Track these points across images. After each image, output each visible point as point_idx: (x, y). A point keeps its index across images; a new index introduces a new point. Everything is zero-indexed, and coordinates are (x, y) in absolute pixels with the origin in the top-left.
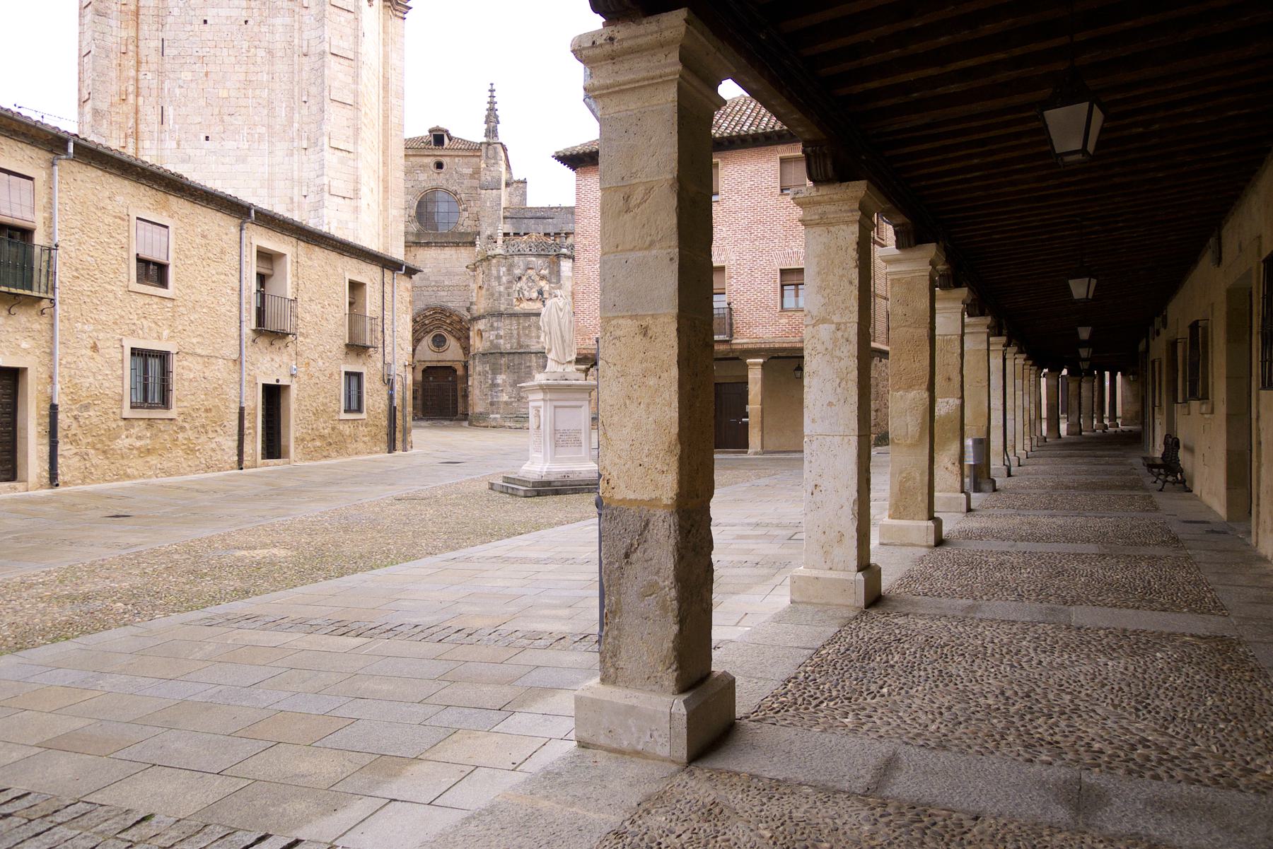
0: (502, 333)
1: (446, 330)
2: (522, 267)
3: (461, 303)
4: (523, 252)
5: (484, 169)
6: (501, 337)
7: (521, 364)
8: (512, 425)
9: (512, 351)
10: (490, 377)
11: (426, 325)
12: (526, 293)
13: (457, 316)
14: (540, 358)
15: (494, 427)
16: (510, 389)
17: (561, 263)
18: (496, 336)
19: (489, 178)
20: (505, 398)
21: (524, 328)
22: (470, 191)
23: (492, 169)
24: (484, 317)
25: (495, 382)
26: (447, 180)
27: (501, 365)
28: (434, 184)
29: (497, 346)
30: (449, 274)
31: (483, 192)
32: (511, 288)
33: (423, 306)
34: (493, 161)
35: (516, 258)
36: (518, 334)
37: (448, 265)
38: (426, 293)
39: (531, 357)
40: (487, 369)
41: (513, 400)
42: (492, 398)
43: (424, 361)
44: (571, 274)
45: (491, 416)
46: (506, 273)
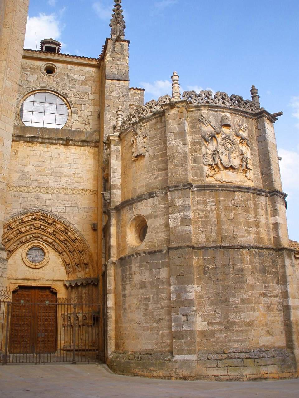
0: (191, 215)
3: (68, 209)
4: (214, 104)
5: (110, 62)
7: (227, 266)
8: (220, 372)
9: (209, 245)
11: (21, 233)
12: (222, 157)
13: (62, 223)
14: (254, 256)
15: (185, 378)
16: (209, 309)
19: (115, 71)
20: (200, 324)
23: (118, 63)
25: (184, 296)
26: (58, 83)
28: (44, 86)
29: (187, 237)
30: (55, 174)
32: (199, 150)
33: (20, 210)
35: (204, 112)
36: (218, 218)
37: (54, 165)
38: (26, 195)
39: (242, 255)
41: (216, 327)
42: (179, 325)
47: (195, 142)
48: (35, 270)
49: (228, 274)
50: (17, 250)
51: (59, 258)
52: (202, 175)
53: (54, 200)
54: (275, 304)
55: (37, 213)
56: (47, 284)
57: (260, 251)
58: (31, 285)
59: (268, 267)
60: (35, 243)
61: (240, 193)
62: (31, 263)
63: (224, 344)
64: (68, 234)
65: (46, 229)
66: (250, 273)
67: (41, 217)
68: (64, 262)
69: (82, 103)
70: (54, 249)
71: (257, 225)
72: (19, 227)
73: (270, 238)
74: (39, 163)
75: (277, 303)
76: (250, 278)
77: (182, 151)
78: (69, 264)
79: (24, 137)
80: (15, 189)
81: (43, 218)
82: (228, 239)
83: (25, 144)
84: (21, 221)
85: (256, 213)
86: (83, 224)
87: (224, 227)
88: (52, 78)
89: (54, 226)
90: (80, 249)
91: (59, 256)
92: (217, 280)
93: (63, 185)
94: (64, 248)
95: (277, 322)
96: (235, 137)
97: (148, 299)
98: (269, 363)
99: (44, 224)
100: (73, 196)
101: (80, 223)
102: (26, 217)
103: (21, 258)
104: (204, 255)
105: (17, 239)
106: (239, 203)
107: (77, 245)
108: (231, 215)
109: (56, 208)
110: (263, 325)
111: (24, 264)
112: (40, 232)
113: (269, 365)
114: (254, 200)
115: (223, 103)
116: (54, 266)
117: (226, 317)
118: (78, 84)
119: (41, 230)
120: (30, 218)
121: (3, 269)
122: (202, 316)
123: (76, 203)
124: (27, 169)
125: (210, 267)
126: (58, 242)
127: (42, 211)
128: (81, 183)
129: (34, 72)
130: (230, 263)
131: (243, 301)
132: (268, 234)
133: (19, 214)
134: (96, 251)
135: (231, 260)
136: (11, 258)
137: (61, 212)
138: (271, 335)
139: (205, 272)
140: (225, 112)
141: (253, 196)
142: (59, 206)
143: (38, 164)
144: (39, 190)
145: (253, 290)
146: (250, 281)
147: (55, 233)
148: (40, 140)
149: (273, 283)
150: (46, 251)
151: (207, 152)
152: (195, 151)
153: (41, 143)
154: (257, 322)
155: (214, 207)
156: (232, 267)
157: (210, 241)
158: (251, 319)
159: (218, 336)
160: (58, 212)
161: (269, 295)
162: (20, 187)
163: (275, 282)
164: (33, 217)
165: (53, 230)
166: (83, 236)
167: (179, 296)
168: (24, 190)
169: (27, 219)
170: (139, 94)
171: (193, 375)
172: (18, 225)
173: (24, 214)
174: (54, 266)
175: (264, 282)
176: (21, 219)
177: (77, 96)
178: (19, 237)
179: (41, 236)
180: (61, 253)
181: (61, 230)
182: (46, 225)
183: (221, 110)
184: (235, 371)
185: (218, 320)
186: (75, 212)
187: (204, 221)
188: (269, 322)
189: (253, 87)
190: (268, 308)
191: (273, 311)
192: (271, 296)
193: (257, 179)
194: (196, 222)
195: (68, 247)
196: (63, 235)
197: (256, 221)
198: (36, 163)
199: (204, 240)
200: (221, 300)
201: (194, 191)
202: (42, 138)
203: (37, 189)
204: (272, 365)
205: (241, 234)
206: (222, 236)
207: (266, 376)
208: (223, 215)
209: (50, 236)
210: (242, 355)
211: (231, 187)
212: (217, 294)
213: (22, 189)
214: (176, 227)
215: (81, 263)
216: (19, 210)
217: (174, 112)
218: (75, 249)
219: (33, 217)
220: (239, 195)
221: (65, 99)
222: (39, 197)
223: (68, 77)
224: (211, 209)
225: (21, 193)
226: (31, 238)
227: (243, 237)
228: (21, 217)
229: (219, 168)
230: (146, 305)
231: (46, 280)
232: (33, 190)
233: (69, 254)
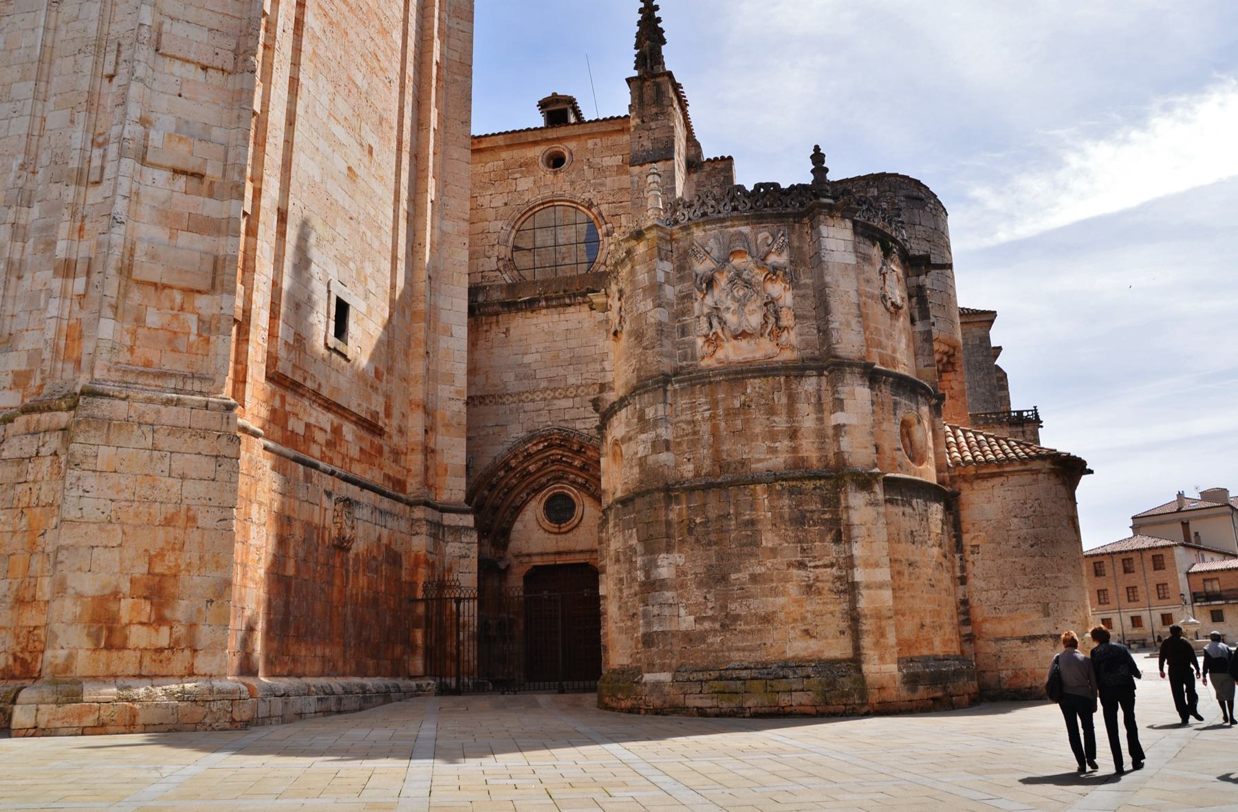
2: (715, 253)
4: (715, 215)
6: (667, 446)
10: (639, 561)
11: (530, 474)
12: (729, 317)
14: (780, 494)
16: (696, 595)
17: (824, 230)
18: (654, 444)
20: (687, 622)
21: (730, 413)
22: (618, 197)
23: (653, 125)
24: (622, 402)
26: (572, 183)
27: (669, 524)
28: (547, 193)
31: (636, 169)
33: (522, 434)
34: (654, 110)
35: (698, 233)
36: (715, 433)
37: (573, 343)
40: (634, 542)
41: (707, 625)
42: (648, 624)
43: (529, 555)
44: (851, 259)
45: (648, 677)
46: (674, 275)
47: (684, 297)
48: (559, 536)
49: (728, 531)
52: (694, 357)
54: (828, 581)
56: (580, 559)
57: (791, 483)
59: (812, 512)
60: (555, 488)
61: (757, 381)
63: (720, 654)
66: (770, 527)
69: (621, 211)
70: (589, 496)
71: (793, 434)
72: (525, 465)
73: (826, 456)
74: (547, 344)
75: (831, 579)
76: (769, 535)
77: (653, 320)
79: (515, 304)
80: (511, 399)
82: (731, 469)
83: (520, 314)
85: (791, 411)
87: (725, 448)
88: (560, 175)
92: (709, 544)
95: (832, 613)
96: (757, 271)
97: (621, 580)
98: (794, 687)
102: (534, 445)
104: (689, 501)
105: (524, 485)
106: (754, 399)
108: (739, 423)
110: (795, 620)
112: (561, 468)
113: (796, 691)
114: (788, 388)
115: (735, 209)
117: (724, 607)
118: (610, 176)
120: (541, 446)
121: (468, 543)
122: (686, 607)
124: (527, 359)
125: (698, 520)
129: (528, 172)
130: (731, 512)
131: (754, 578)
132: (820, 449)
135: (732, 507)
136: (519, 519)
138: (814, 637)
139: (690, 531)
140: (738, 226)
141: (786, 382)
143: (545, 348)
144: (552, 394)
145: (774, 558)
146: (769, 540)
148: (543, 303)
149: (822, 540)
150: (576, 500)
151: (702, 311)
152: (683, 314)
153: (547, 307)
154: (782, 615)
155: (707, 414)
156: (733, 517)
157: (700, 475)
158: (770, 609)
159: (710, 640)
161: (812, 564)
162: (519, 394)
163: (829, 538)
167: (647, 575)
168: (527, 397)
169: (535, 448)
170: (722, 170)
171: (667, 705)
173: (530, 440)
175: (800, 542)
176: (526, 450)
177: (611, 199)
179: (565, 476)
183: (729, 223)
184: (730, 700)
185: (710, 613)
187: (692, 440)
188: (809, 615)
189: (817, 148)
190: (809, 589)
191: (820, 594)
192: (816, 567)
193: (807, 344)
194: (679, 444)
197: (789, 428)
198: (542, 346)
199: (691, 475)
200: (714, 578)
201: (675, 390)
202: (547, 299)
203: (549, 392)
204: (802, 690)
205: (757, 456)
206: (721, 464)
207: (788, 710)
208: (723, 425)
209: (580, 473)
210: (744, 674)
211: (737, 372)
212: (709, 568)
213: (523, 398)
214: (646, 456)
216: (520, 435)
217: (641, 248)
220: (754, 386)
221: (590, 210)
223: (590, 167)
224: (703, 418)
225: (521, 404)
226: (548, 481)
227: (760, 461)
229: (722, 340)
230: (621, 590)
232: (541, 396)
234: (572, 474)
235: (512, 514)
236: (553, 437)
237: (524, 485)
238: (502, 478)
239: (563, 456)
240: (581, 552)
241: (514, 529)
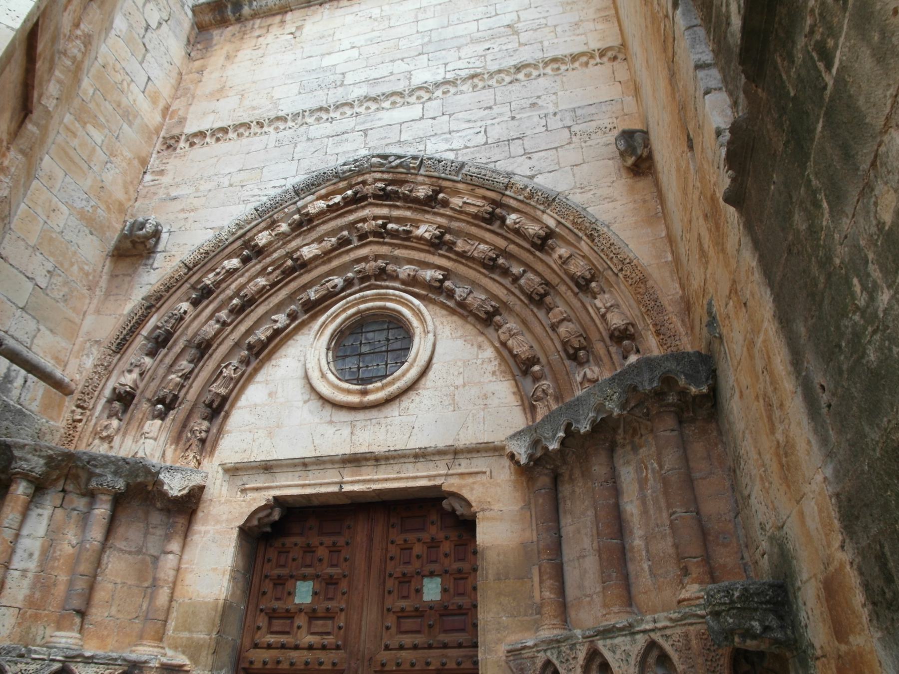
1: (412, 282)
11: (303, 265)
33: (299, 178)
43: (268, 468)
48: (361, 415)
50: (291, 342)
51: (480, 347)
53: (434, 118)
55: (367, 177)
58: (335, 489)
62: (346, 385)
64: (508, 222)
65: (408, 228)
67: (380, 185)
68: (506, 362)
70: (452, 312)
72: (294, 244)
74: (377, 34)
78: (534, 361)
81: (389, 188)
84: (296, 217)
86: (576, 165)
89: (442, 211)
90: (578, 267)
91: (481, 339)
93: (470, 66)
94: (501, 292)
99: (396, 213)
100: (516, 87)
101: (559, 163)
103: (300, 373)
105: (283, 294)
107: (560, 257)
109: (442, 140)
111: (313, 396)
116: (459, 382)
119: (387, 240)
123: (533, 105)
126: (471, 274)
127: (385, 162)
128: (546, 44)
133: (287, 192)
134: (670, 258)
136: (260, 377)
137: (468, 147)
142: (458, 131)
147: (448, 237)
150: (415, 323)
160: (452, 150)
164: (349, 192)
165: (439, 227)
166: (585, 209)
169: (322, 204)
172: (284, 235)
174: (459, 382)
176: (298, 211)
178: (293, 286)
180: (484, 316)
181: (473, 210)
182: (408, 214)
186: (529, 133)
195: (516, 279)
196: (488, 236)
215: (594, 336)
218: (555, 280)
219: (349, 192)
222: (373, 123)
228: (300, 204)
231: (416, 456)
233: (526, 313)
234: (410, 261)
235: (246, 362)
236: (369, 178)
237: (283, 294)
238: (231, 273)
239: (389, 219)
240: (421, 455)
241: (243, 401)
